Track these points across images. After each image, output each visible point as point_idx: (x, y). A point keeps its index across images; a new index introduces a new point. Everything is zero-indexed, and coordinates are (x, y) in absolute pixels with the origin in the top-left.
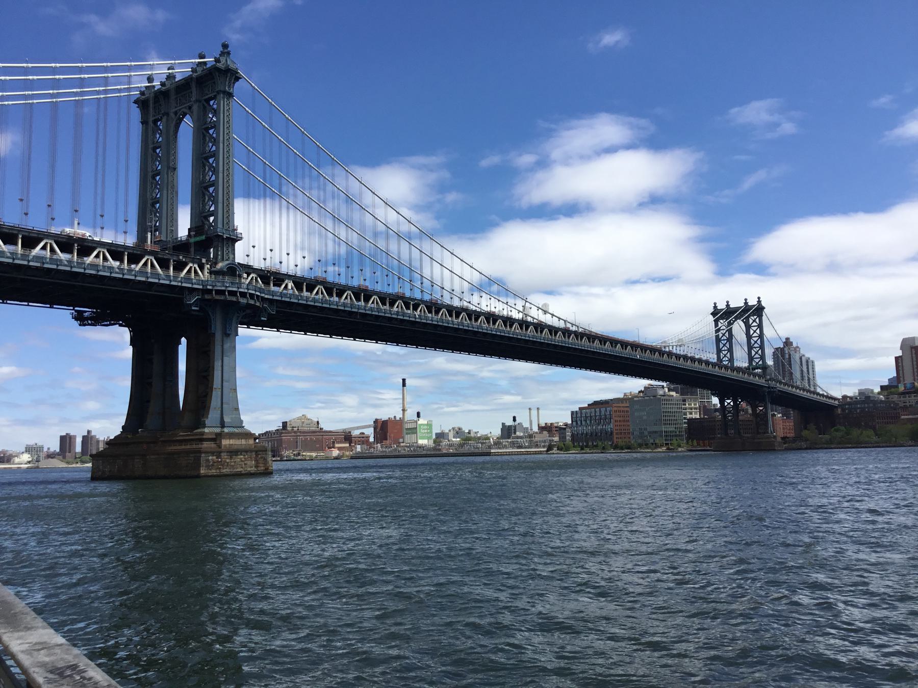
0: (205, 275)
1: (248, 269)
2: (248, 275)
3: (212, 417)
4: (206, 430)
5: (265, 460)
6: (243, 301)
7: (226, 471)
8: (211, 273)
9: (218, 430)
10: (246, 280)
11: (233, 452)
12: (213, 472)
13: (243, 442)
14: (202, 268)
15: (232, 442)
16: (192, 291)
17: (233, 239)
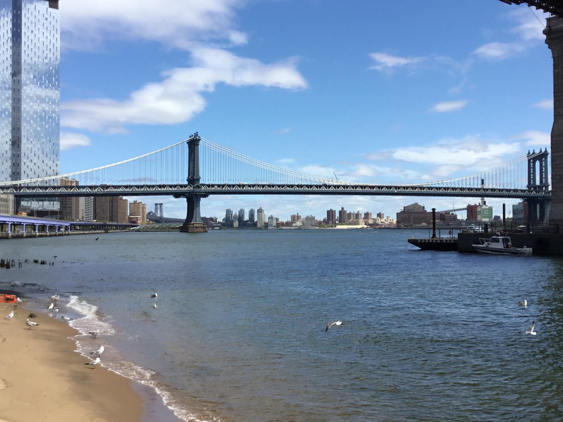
0: (192, 189)
1: (203, 185)
2: (203, 186)
3: (194, 219)
4: (192, 222)
5: (205, 229)
6: (198, 194)
7: (194, 231)
8: (193, 187)
9: (195, 222)
10: (203, 188)
11: (197, 227)
12: (192, 231)
13: (200, 225)
14: (191, 187)
15: (196, 225)
16: (187, 193)
17: (198, 180)
